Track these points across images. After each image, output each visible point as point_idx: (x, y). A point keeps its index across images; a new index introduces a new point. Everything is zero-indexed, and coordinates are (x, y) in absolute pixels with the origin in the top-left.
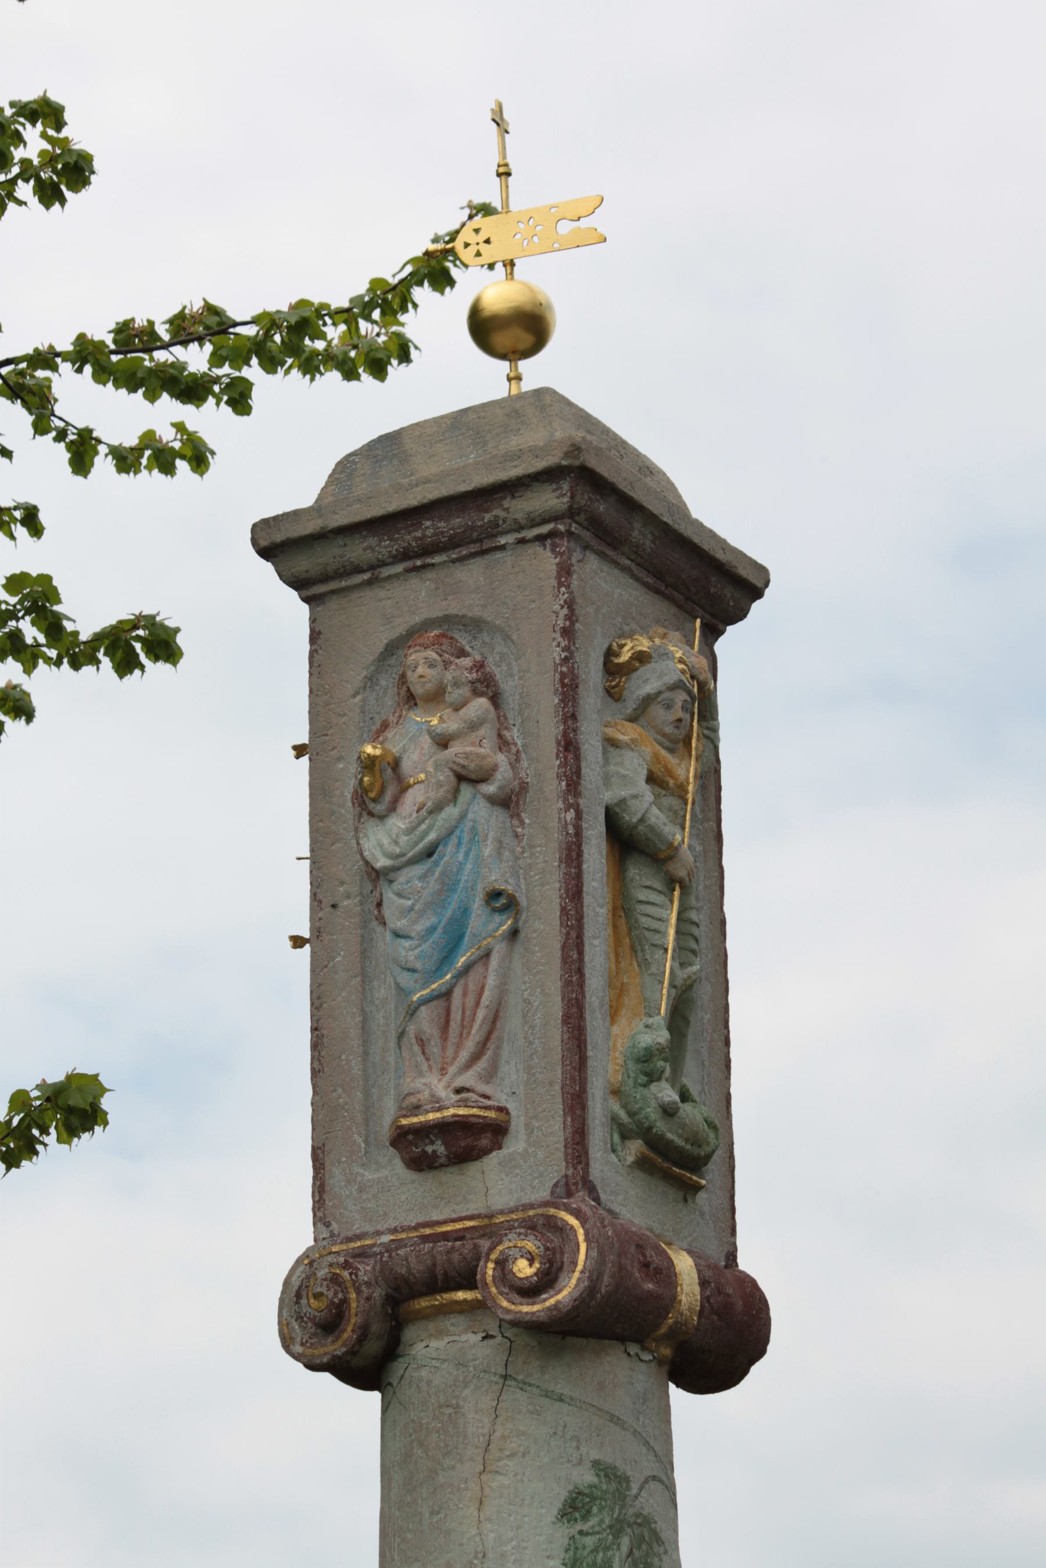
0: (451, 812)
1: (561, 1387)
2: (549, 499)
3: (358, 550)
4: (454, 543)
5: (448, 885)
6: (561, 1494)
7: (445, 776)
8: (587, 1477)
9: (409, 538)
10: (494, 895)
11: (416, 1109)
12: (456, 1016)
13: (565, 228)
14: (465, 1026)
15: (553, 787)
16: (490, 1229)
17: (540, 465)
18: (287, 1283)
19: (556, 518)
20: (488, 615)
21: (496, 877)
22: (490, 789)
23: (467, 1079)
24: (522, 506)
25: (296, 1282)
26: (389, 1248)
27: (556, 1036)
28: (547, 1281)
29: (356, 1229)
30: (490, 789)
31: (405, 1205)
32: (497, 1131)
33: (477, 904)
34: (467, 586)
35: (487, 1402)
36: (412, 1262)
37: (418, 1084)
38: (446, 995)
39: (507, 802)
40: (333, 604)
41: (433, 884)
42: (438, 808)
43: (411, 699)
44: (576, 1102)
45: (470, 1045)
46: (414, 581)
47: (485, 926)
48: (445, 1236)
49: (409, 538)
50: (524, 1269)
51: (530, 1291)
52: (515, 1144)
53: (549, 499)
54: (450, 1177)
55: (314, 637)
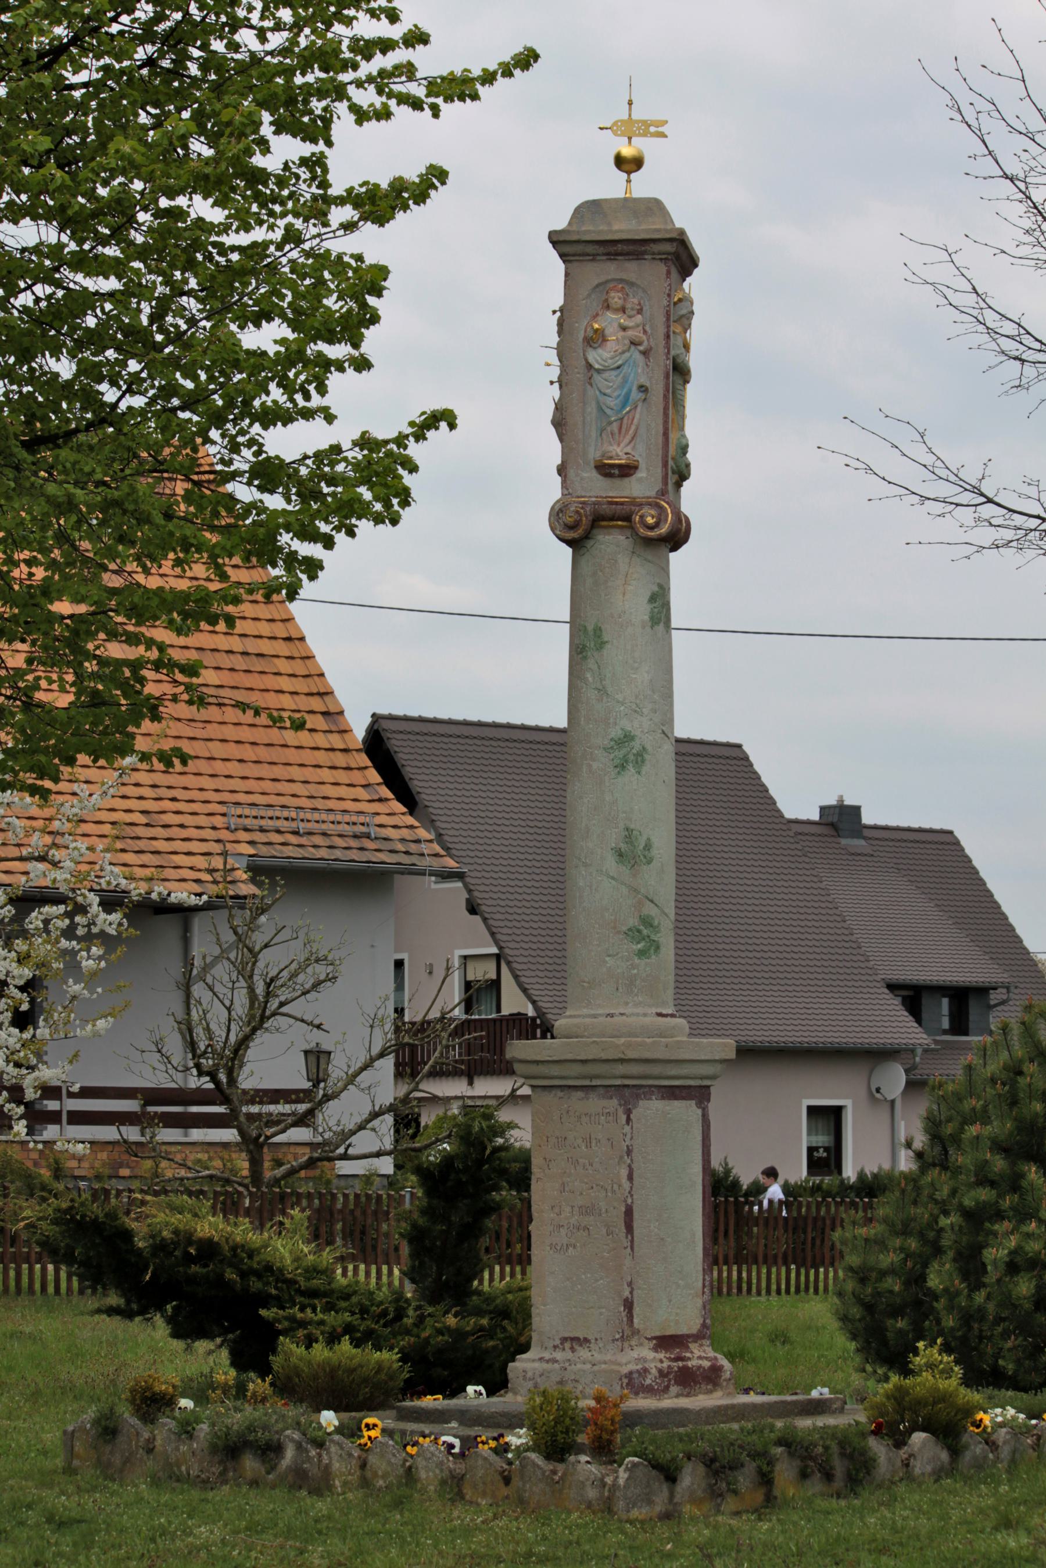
0: (627, 355)
1: (650, 558)
2: (669, 248)
3: (590, 249)
4: (628, 254)
5: (625, 380)
6: (649, 594)
7: (627, 342)
8: (656, 589)
9: (612, 249)
10: (641, 386)
11: (611, 458)
12: (624, 427)
13: (652, 129)
14: (627, 431)
15: (662, 350)
16: (634, 502)
17: (668, 236)
18: (553, 508)
19: (668, 254)
20: (638, 282)
21: (643, 380)
22: (641, 348)
23: (628, 449)
24: (656, 248)
25: (557, 508)
26: (594, 503)
27: (660, 439)
28: (657, 525)
29: (579, 493)
30: (641, 348)
31: (597, 489)
32: (636, 468)
33: (635, 388)
34: (630, 270)
35: (627, 560)
36: (606, 509)
37: (611, 448)
38: (622, 419)
39: (645, 353)
40: (575, 264)
41: (620, 379)
42: (623, 352)
43: (608, 307)
44: (665, 464)
45: (628, 438)
46: (609, 263)
47: (635, 395)
48: (617, 503)
49: (612, 249)
50: (650, 520)
51: (651, 528)
52: (641, 474)
53: (669, 248)
54: (617, 482)
55: (567, 275)
